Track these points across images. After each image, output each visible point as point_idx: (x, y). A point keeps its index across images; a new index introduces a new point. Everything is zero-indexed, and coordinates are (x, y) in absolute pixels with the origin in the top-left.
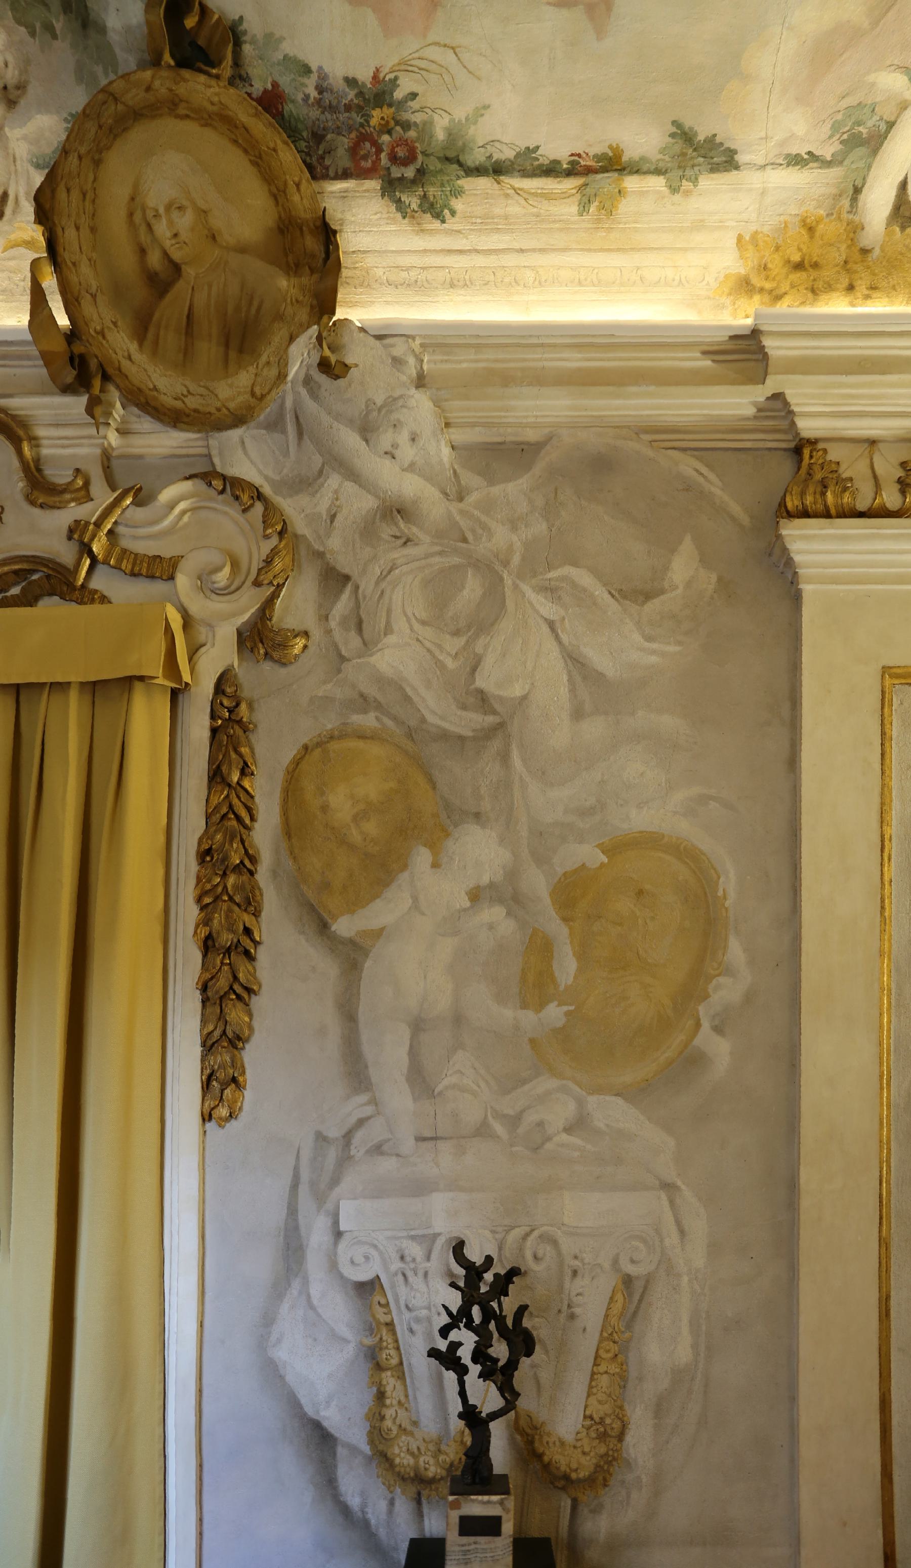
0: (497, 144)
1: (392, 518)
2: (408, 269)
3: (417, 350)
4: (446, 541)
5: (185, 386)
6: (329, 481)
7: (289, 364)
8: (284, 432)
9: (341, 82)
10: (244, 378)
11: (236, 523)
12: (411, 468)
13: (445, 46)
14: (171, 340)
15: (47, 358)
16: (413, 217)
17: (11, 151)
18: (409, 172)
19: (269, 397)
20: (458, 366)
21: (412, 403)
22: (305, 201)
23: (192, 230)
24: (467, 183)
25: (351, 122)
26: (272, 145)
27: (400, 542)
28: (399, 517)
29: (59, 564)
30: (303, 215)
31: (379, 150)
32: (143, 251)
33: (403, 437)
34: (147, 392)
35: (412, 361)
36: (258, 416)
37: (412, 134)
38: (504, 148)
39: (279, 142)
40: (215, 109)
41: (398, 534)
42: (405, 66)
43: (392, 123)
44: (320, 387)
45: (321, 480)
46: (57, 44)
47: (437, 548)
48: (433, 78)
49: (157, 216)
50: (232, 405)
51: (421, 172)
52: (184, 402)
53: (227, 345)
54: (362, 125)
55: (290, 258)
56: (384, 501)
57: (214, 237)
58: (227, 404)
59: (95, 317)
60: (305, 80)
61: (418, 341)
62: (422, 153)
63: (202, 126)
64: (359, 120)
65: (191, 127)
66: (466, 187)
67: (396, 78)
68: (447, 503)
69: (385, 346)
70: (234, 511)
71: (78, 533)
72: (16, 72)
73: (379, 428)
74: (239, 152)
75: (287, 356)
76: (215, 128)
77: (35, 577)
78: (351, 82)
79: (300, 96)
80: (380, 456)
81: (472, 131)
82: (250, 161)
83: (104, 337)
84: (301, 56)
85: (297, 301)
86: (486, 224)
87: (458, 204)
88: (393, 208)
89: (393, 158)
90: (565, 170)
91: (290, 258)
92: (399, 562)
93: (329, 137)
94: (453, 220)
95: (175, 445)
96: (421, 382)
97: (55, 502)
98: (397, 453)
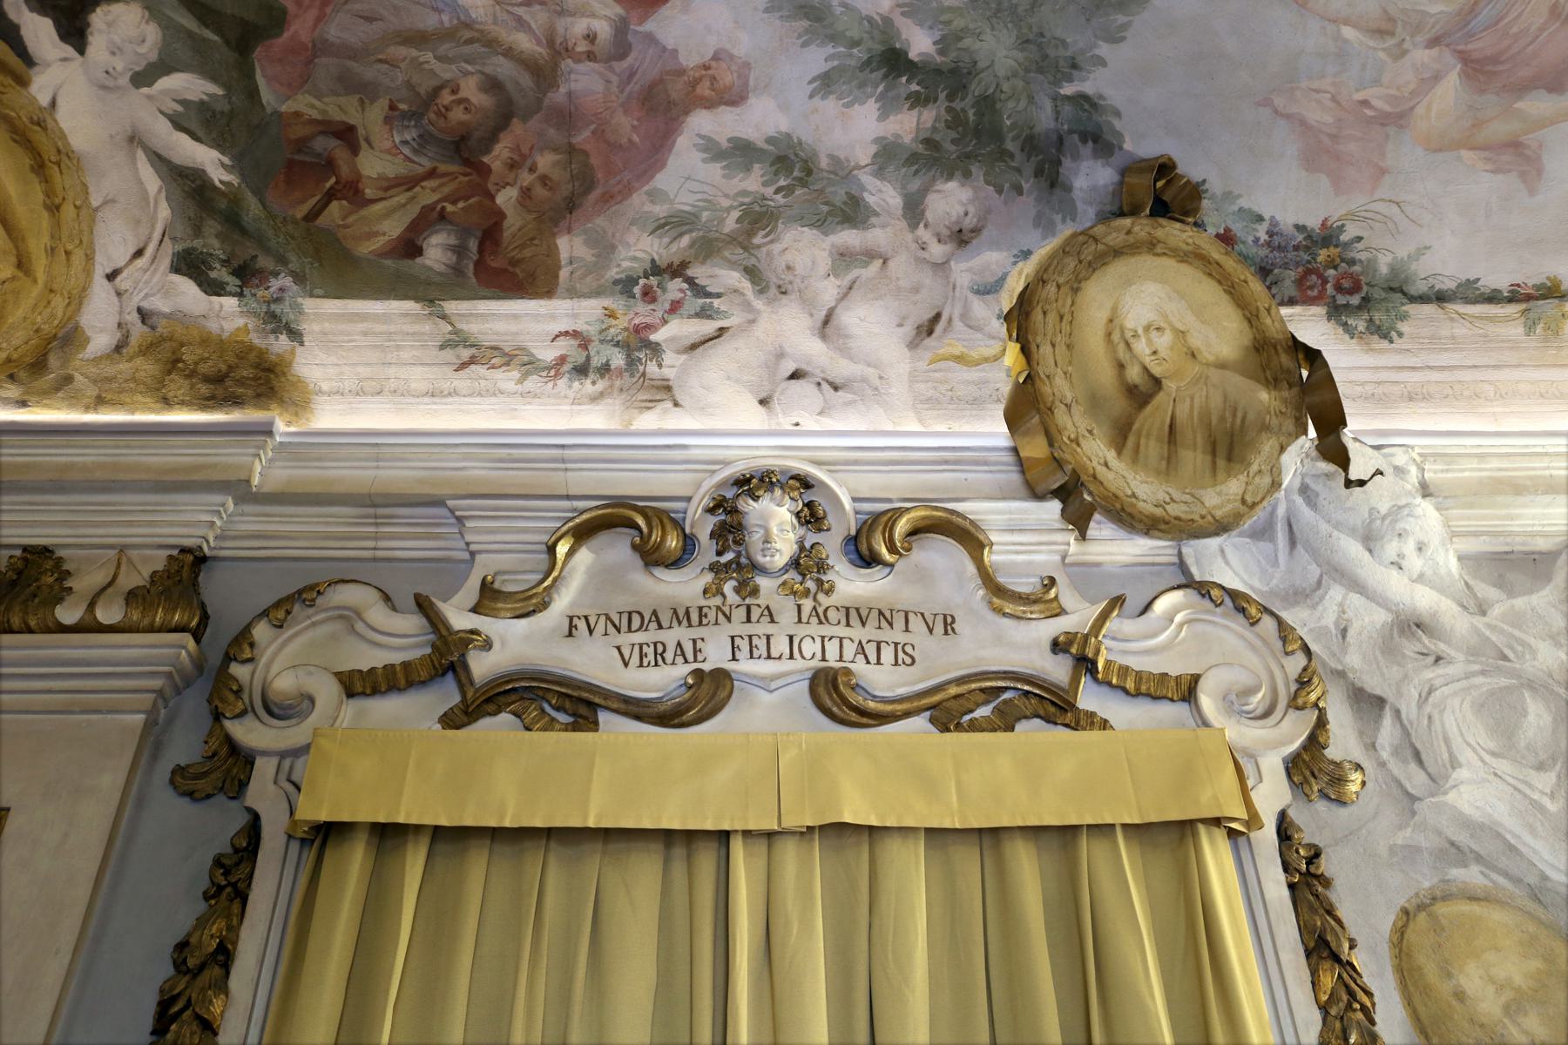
0: (1440, 278)
1: (1413, 634)
2: (1363, 384)
3: (1418, 459)
4: (1484, 659)
5: (1168, 493)
6: (1331, 593)
7: (1283, 473)
8: (1272, 539)
9: (1291, 228)
10: (1234, 487)
11: (1242, 637)
12: (1420, 579)
13: (1390, 201)
14: (1153, 449)
15: (1021, 464)
16: (1361, 338)
17: (952, 280)
18: (1355, 300)
19: (1261, 506)
20: (1460, 475)
21: (1419, 511)
22: (1276, 323)
23: (1172, 348)
24: (1412, 309)
25: (1298, 259)
26: (1242, 277)
27: (1431, 659)
28: (1420, 632)
29: (1045, 681)
30: (1275, 335)
31: (1325, 282)
32: (1121, 366)
33: (1409, 547)
34: (1125, 498)
35: (1413, 470)
36: (1244, 523)
37: (1357, 268)
38: (1446, 280)
39: (1248, 275)
40: (1190, 248)
41: (1425, 651)
42: (1352, 216)
43: (1338, 260)
44: (1317, 495)
45: (1321, 592)
46: (1024, 198)
47: (1476, 667)
48: (1377, 226)
49: (1136, 336)
50: (1219, 514)
51: (1366, 300)
52: (1165, 510)
53: (1214, 453)
54: (1309, 262)
55: (1268, 373)
56: (1397, 614)
57: (1193, 355)
58: (1213, 512)
59: (1069, 425)
60: (1257, 226)
61: (1417, 450)
62: (1367, 284)
63: (1179, 261)
64: (1306, 257)
65: (1169, 263)
66: (1411, 313)
67: (1343, 226)
68: (1469, 616)
69: (1385, 456)
70: (1237, 624)
71: (1075, 646)
72: (975, 220)
73: (1382, 538)
74: (1214, 283)
75: (1280, 464)
76: (1190, 264)
77: (1007, 695)
78: (1300, 228)
79: (1250, 239)
80: (1386, 567)
81: (1414, 266)
82: (1224, 290)
83: (1078, 445)
84: (1256, 208)
85: (1280, 412)
86: (1435, 344)
87: (1404, 327)
88: (1340, 330)
89: (1339, 288)
90: (1506, 297)
91: (1268, 373)
92: (1437, 682)
93: (1276, 271)
94: (1400, 341)
95: (1139, 552)
96: (1425, 490)
97: (1024, 612)
98: (1404, 563)
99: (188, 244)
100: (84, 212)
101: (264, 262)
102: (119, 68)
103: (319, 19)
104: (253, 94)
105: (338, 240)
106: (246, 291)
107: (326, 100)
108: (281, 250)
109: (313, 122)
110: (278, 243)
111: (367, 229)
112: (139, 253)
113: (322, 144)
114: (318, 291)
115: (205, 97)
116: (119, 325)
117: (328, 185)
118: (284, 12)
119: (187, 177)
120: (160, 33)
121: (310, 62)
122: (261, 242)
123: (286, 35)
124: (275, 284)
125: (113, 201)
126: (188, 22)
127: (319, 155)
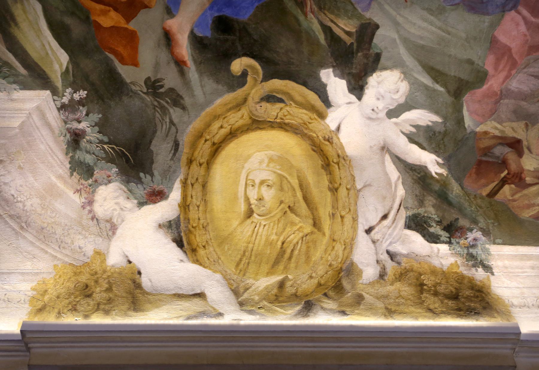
99: (415, 211)
100: (352, 192)
101: (463, 222)
102: (380, 107)
103: (507, 77)
104: (460, 121)
105: (509, 209)
106: (453, 240)
107: (504, 124)
108: (474, 215)
109: (495, 137)
110: (471, 210)
111: (527, 202)
112: (385, 217)
113: (499, 151)
114: (498, 241)
115: (430, 124)
116: (378, 261)
117: (503, 175)
118: (486, 74)
119: (415, 170)
120: (408, 87)
121: (497, 102)
122: (461, 210)
123: (485, 87)
124: (471, 236)
125: (370, 185)
126: (426, 80)
127: (498, 158)
